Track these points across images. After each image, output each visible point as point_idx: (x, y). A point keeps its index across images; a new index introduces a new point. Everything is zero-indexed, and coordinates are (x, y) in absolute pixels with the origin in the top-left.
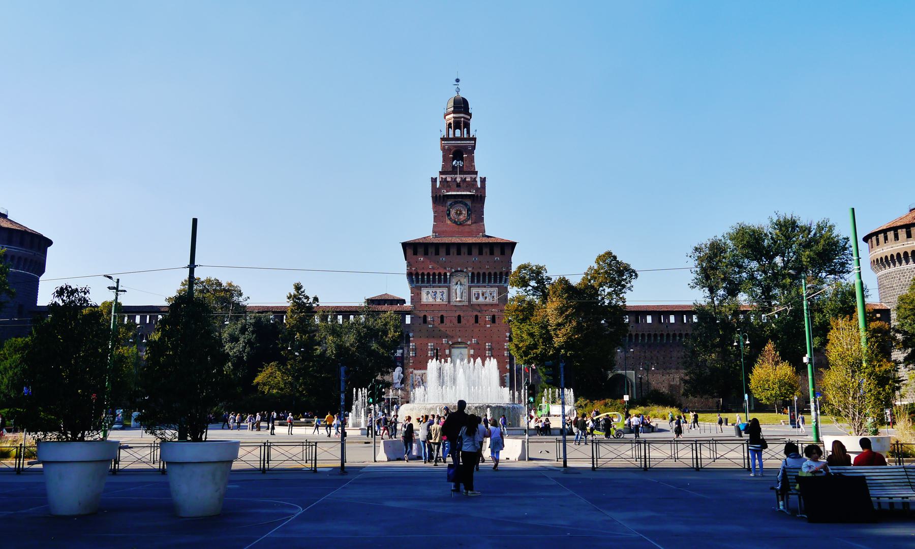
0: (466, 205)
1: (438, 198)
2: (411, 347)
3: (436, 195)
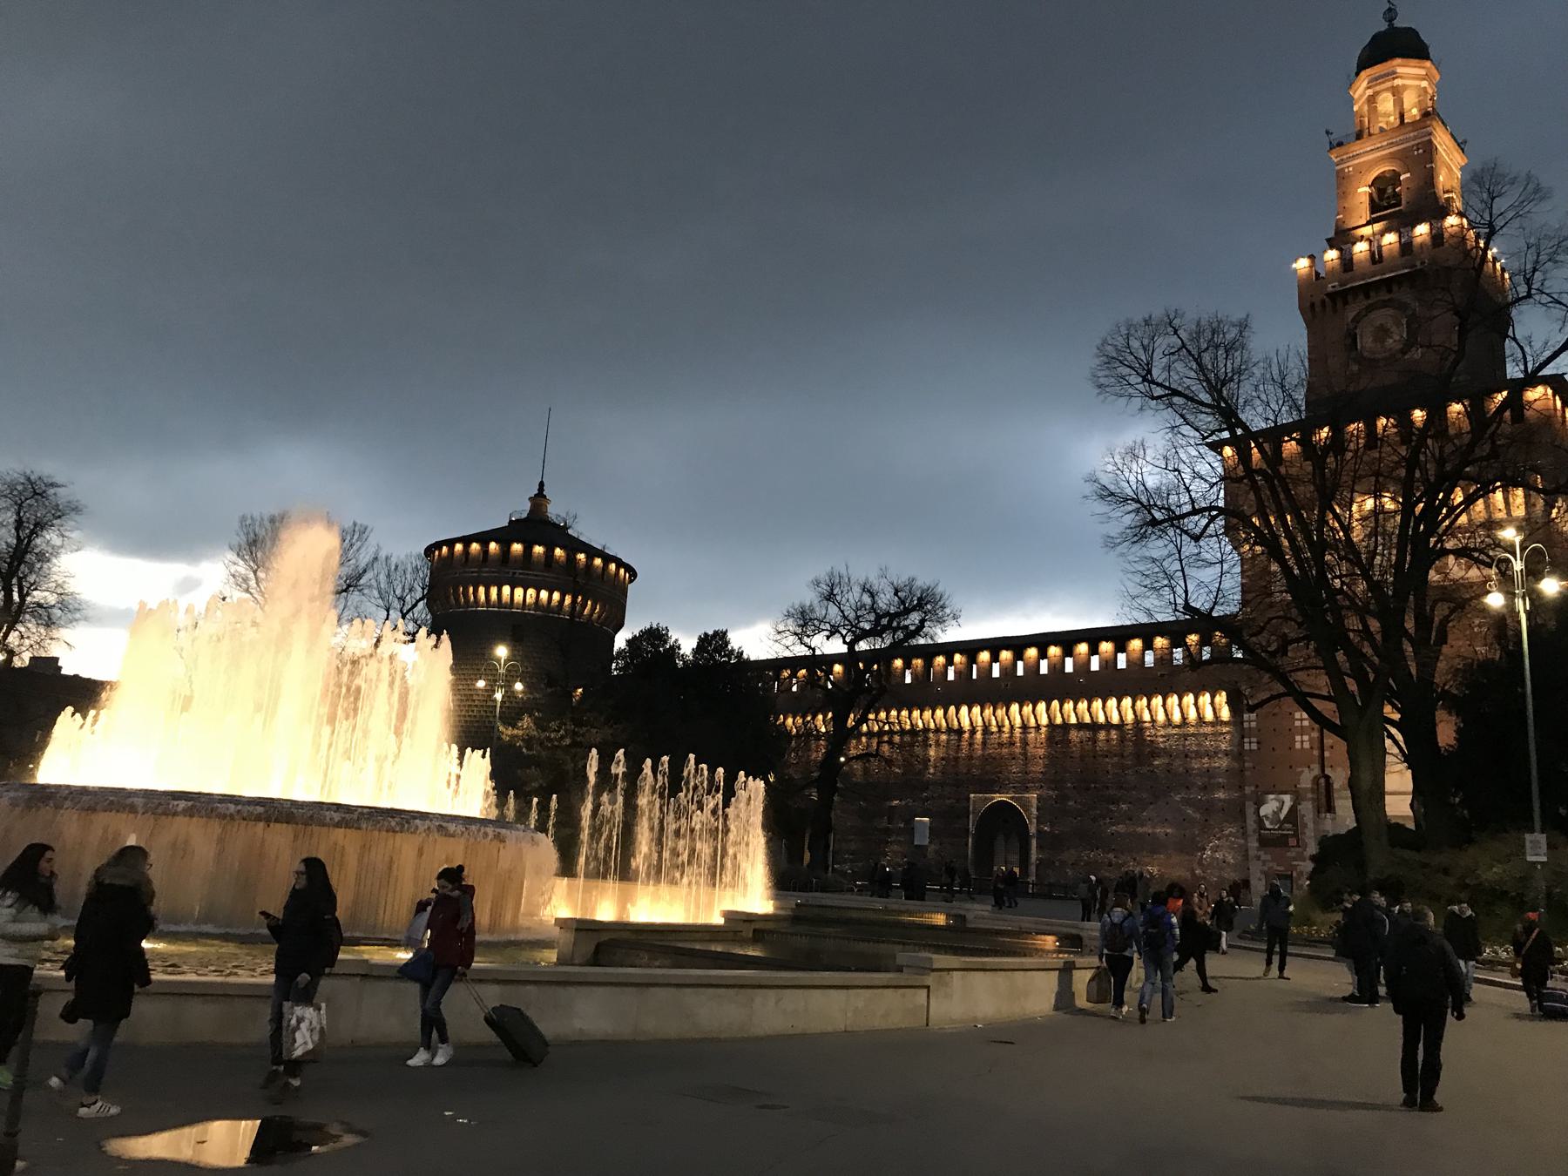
0: (1402, 307)
1: (1318, 308)
2: (1246, 725)
3: (1313, 305)
